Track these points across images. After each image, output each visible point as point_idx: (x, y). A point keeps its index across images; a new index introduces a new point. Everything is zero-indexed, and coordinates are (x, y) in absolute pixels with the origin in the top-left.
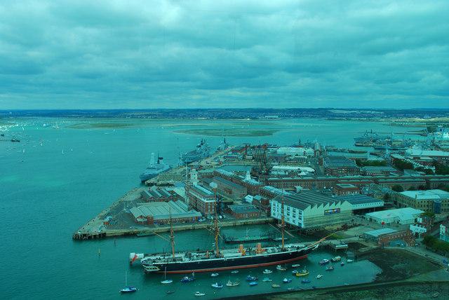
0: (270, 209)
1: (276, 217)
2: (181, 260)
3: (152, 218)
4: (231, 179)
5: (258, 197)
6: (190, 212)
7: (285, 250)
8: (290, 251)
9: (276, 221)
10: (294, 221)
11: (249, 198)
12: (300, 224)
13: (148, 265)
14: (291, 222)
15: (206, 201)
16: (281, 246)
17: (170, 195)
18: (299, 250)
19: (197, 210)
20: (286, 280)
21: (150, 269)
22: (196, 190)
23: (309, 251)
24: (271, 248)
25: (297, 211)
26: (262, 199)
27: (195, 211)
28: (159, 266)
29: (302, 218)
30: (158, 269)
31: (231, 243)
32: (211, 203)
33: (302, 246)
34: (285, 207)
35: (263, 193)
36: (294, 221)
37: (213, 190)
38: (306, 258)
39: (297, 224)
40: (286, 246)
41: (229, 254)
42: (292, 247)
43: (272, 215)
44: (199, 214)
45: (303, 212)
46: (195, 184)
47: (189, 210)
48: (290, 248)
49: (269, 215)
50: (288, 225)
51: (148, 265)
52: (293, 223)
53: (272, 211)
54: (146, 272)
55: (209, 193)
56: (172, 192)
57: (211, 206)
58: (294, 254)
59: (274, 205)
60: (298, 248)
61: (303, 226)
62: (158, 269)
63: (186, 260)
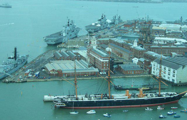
0: (151, 68)
1: (155, 74)
2: (82, 99)
3: (61, 71)
4: (122, 45)
5: (142, 60)
6: (90, 68)
7: (161, 96)
8: (164, 96)
9: (154, 76)
10: (169, 78)
11: (135, 60)
12: (173, 80)
13: (57, 102)
14: (166, 78)
15: (102, 60)
16: (158, 93)
17: (75, 55)
18: (172, 96)
19: (95, 67)
20: (161, 116)
21: (59, 104)
22: (95, 52)
23: (179, 97)
24: (150, 94)
25: (172, 70)
26: (145, 61)
27: (94, 68)
28: (66, 103)
29: (175, 76)
30: (65, 105)
31: (119, 89)
32: (106, 62)
33: (174, 93)
34: (163, 67)
35: (146, 56)
36: (169, 78)
37: (109, 52)
38: (177, 103)
39: (171, 80)
40: (162, 93)
41: (118, 96)
42: (166, 94)
43: (152, 73)
44: (96, 70)
45: (176, 71)
46: (94, 47)
47: (89, 67)
48: (164, 95)
49: (150, 73)
50: (165, 80)
51: (57, 102)
52: (168, 80)
53: (153, 70)
54: (56, 107)
55: (105, 54)
56: (77, 54)
57: (106, 64)
58: (168, 100)
59: (154, 65)
60: (171, 95)
61: (175, 82)
62: (65, 105)
63: (86, 100)
